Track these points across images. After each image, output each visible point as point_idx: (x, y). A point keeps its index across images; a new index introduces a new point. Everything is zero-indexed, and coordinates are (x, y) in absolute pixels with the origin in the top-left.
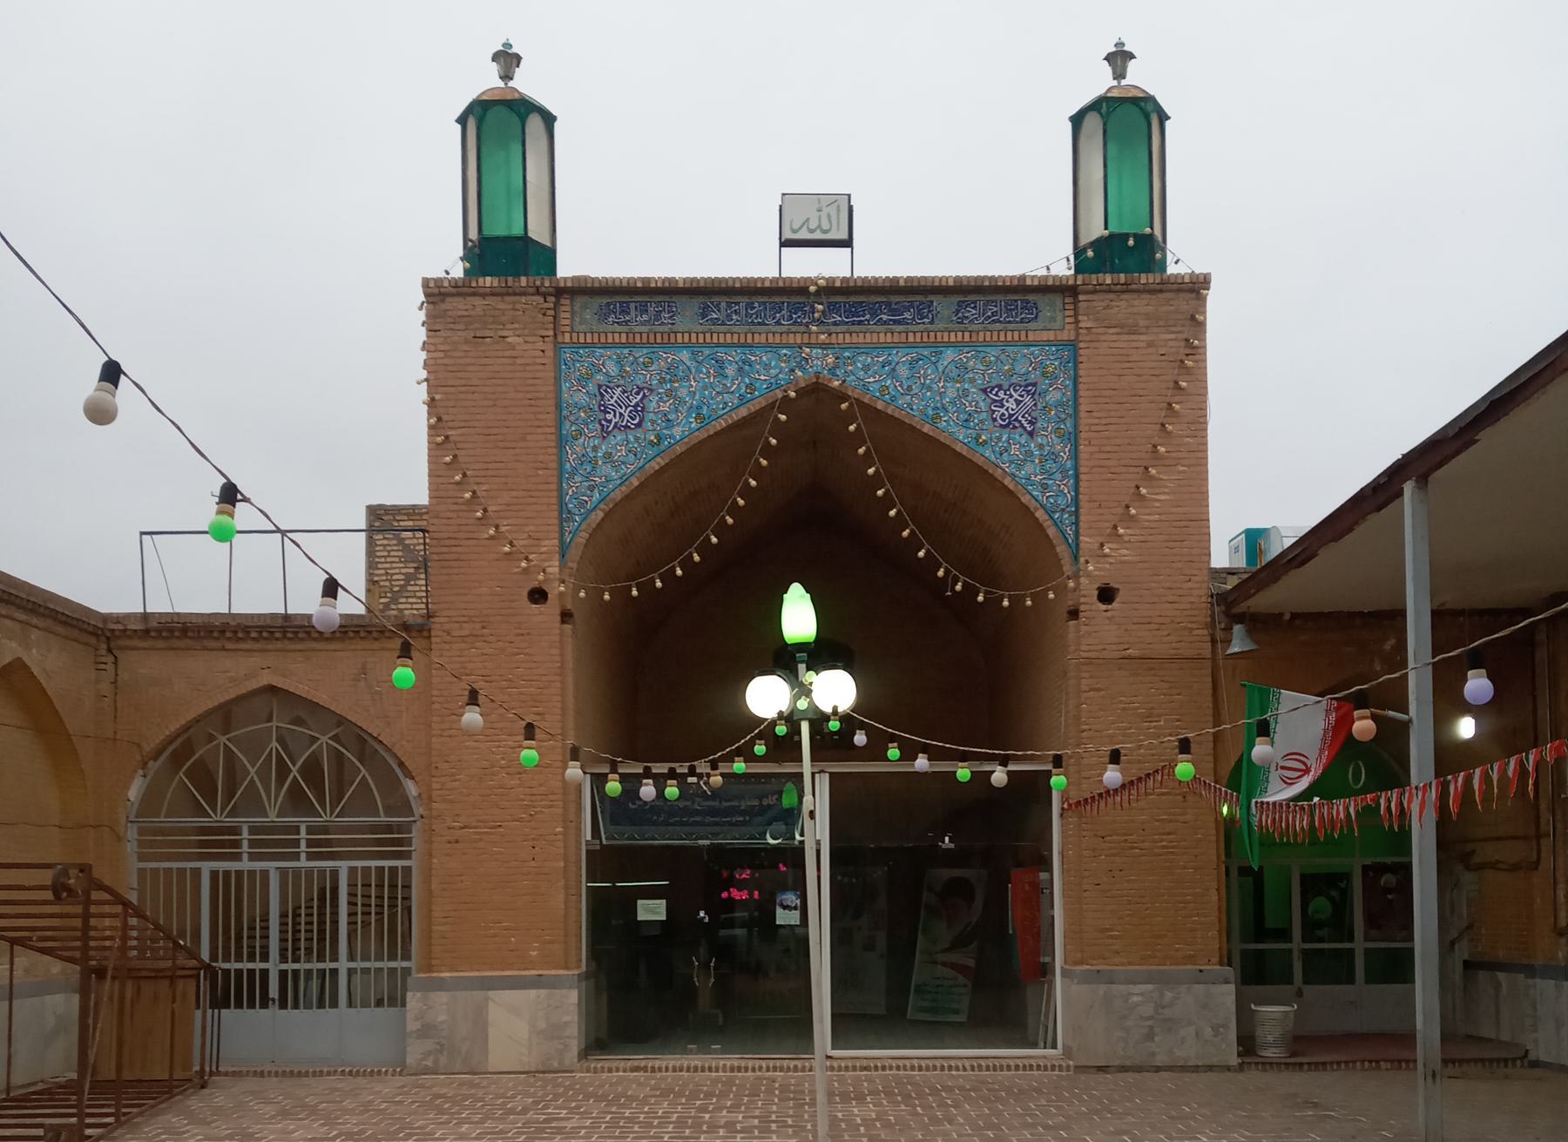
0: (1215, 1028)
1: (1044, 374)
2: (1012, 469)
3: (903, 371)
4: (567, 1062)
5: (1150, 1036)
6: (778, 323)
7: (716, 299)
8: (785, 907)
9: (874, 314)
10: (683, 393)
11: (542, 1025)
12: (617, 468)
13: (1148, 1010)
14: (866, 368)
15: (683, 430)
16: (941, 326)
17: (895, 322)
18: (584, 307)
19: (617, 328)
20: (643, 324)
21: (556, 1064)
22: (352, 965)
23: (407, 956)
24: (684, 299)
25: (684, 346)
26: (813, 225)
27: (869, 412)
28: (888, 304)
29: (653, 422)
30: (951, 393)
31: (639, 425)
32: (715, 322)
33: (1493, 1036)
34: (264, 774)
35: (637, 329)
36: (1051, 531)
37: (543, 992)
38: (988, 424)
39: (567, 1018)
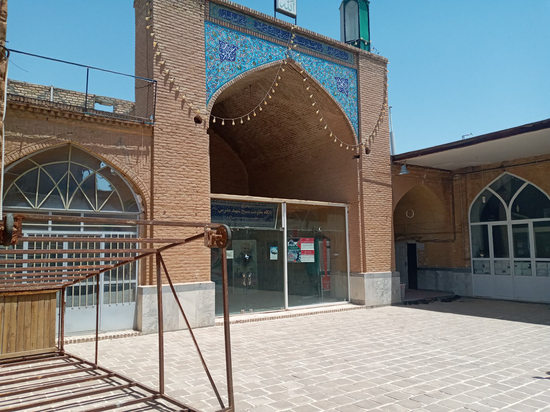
0: (396, 291)
1: (350, 77)
2: (343, 106)
3: (314, 65)
4: (211, 322)
5: (382, 295)
6: (279, 37)
7: (260, 21)
8: (274, 253)
9: (306, 43)
10: (249, 52)
11: (201, 306)
12: (226, 73)
13: (381, 287)
14: (304, 61)
15: (249, 67)
16: (324, 53)
17: (312, 48)
18: (214, 8)
19: (226, 21)
20: (235, 22)
21: (206, 323)
22: (107, 282)
23: (134, 277)
24: (249, 17)
25: (248, 35)
26: (287, 7)
27: (304, 75)
28: (310, 41)
29: (239, 60)
30: (327, 77)
31: (234, 60)
32: (259, 29)
33: (434, 289)
34: (63, 186)
35: (233, 23)
36: (353, 128)
37: (201, 291)
38: (337, 90)
39: (211, 302)
